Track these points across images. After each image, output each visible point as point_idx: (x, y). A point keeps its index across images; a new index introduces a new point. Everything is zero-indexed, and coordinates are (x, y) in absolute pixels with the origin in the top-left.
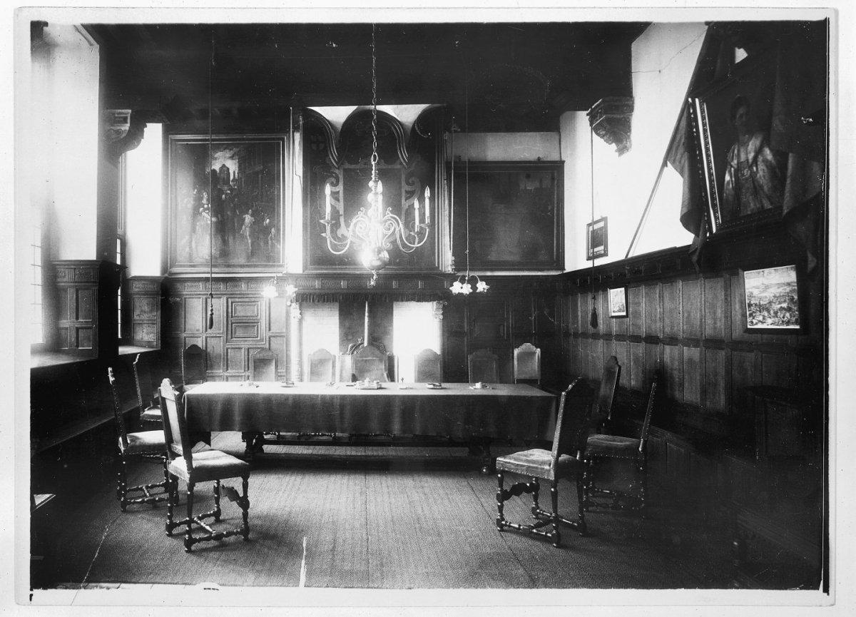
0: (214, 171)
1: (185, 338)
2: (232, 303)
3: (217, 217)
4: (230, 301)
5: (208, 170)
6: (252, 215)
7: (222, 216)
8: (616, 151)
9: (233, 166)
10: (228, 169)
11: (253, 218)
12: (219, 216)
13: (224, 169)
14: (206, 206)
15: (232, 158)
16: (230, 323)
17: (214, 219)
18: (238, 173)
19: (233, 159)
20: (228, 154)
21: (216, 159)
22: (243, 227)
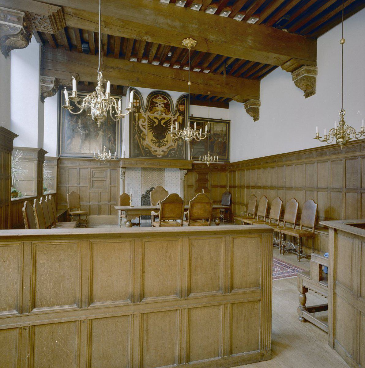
1: (69, 187)
2: (93, 171)
4: (91, 170)
8: (304, 96)
14: (80, 126)
17: (84, 132)
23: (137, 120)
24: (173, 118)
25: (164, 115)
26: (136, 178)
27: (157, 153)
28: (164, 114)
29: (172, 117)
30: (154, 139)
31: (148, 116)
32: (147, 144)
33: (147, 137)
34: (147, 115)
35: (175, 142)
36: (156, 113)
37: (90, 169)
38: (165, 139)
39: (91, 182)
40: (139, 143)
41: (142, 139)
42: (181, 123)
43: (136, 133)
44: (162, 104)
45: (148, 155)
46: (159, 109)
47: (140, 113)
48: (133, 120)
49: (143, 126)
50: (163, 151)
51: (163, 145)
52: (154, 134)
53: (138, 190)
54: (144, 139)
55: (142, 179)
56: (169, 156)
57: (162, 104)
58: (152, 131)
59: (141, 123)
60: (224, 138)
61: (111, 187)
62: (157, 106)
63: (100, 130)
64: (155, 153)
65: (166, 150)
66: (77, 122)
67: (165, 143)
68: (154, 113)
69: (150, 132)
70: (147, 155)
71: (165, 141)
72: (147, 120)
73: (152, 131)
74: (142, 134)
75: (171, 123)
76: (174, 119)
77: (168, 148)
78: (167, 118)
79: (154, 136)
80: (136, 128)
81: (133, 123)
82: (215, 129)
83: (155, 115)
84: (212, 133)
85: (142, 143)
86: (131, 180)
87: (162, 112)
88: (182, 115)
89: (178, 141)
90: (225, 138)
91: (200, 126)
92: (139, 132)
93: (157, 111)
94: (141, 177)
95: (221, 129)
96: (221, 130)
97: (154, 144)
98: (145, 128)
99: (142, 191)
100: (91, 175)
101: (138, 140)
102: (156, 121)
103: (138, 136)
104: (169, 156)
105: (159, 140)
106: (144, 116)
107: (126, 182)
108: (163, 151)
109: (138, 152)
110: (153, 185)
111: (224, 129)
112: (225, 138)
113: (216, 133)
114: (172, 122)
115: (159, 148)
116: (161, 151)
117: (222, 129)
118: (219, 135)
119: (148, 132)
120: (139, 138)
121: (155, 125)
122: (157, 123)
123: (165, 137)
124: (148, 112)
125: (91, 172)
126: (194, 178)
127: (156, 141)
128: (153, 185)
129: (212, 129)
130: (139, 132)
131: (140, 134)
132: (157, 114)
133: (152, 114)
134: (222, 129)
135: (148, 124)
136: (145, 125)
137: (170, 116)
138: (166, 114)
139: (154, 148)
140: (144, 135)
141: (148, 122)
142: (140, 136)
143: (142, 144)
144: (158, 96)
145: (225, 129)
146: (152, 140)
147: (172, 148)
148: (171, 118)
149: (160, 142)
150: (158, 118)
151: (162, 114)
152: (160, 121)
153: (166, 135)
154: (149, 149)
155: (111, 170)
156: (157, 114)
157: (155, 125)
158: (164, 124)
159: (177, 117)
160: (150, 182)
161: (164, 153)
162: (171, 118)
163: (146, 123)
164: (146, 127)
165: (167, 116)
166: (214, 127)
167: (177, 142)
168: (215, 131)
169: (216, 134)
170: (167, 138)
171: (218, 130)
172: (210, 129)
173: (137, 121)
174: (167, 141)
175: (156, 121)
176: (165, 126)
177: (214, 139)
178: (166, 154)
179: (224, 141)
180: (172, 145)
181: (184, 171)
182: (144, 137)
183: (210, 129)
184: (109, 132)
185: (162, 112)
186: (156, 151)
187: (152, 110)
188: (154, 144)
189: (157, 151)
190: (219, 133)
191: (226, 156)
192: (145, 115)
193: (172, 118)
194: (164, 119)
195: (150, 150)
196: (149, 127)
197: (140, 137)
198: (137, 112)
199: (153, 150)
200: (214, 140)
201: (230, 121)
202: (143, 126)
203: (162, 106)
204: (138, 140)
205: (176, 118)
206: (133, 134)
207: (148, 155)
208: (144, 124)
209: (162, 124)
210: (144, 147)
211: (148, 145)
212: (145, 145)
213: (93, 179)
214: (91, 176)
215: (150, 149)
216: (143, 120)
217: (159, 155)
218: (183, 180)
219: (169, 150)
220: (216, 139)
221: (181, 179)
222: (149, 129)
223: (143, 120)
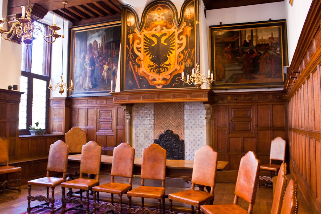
0: (91, 44)
2: (99, 111)
3: (92, 67)
4: (98, 110)
5: (88, 43)
6: (108, 65)
7: (94, 67)
9: (99, 41)
10: (97, 42)
11: (108, 67)
12: (93, 67)
13: (96, 42)
14: (87, 62)
15: (99, 36)
16: (98, 122)
17: (90, 69)
18: (102, 44)
19: (99, 37)
20: (97, 34)
21: (91, 38)
22: (103, 71)
23: (131, 42)
24: (178, 31)
25: (165, 30)
27: (156, 82)
28: (164, 28)
29: (176, 30)
30: (152, 63)
31: (144, 35)
32: (143, 72)
33: (142, 63)
34: (143, 34)
35: (182, 64)
36: (154, 29)
37: (97, 108)
38: (167, 63)
39: (98, 123)
40: (134, 72)
41: (136, 66)
42: (189, 35)
43: (130, 60)
44: (162, 15)
45: (145, 86)
46: (159, 23)
47: (135, 33)
48: (127, 44)
49: (138, 49)
50: (164, 79)
51: (164, 70)
52: (152, 57)
53: (149, 134)
54: (139, 66)
55: (154, 120)
56: (173, 85)
57: (162, 15)
58: (150, 54)
59: (135, 45)
60: (277, 49)
62: (156, 20)
63: (105, 64)
64: (153, 82)
65: (169, 77)
66: (84, 58)
67: (166, 68)
68: (151, 30)
69: (147, 55)
70: (143, 86)
71: (167, 65)
72: (143, 41)
73: (150, 54)
74: (137, 59)
75: (175, 39)
76: (179, 32)
77: (171, 74)
78: (169, 33)
79: (152, 60)
80: (130, 52)
81: (127, 48)
82: (260, 38)
83: (153, 32)
84: (254, 44)
85: (136, 71)
87: (162, 26)
88: (190, 25)
89: (185, 62)
90: (278, 49)
91: (235, 36)
92: (134, 58)
93: (156, 26)
95: (270, 36)
96: (270, 38)
97: (152, 71)
98: (140, 52)
99: (154, 135)
101: (132, 68)
102: (154, 39)
103: (132, 63)
104: (173, 85)
105: (159, 64)
106: (140, 36)
108: (164, 79)
109: (132, 84)
110: (169, 126)
111: (276, 35)
112: (278, 49)
113: (261, 43)
114: (176, 37)
115: (159, 75)
116: (161, 79)
117: (272, 35)
118: (267, 45)
119: (144, 56)
120: (133, 65)
121: (153, 45)
122: (156, 43)
123: (166, 59)
124: (145, 30)
126: (227, 117)
127: (154, 66)
128: (169, 126)
129: (254, 39)
130: (134, 58)
131: (135, 60)
132: (156, 30)
133: (150, 32)
134: (272, 35)
135: (145, 46)
136: (140, 48)
137: (173, 29)
138: (167, 28)
139: (152, 75)
140: (140, 60)
141: (144, 42)
142: (135, 62)
143: (137, 73)
144: (157, 7)
145: (277, 36)
146: (149, 66)
147: (176, 73)
148: (174, 32)
149: (159, 67)
150: (157, 34)
151: (162, 29)
152: (159, 39)
153: (168, 56)
154: (144, 78)
156: (156, 30)
157: (153, 45)
158: (165, 41)
159: (183, 29)
160: (165, 123)
161: (165, 81)
162: (174, 32)
163: (142, 45)
164: (142, 50)
165: (169, 30)
166: (257, 34)
167: (183, 63)
168: (260, 40)
169: (262, 45)
170: (170, 60)
171: (264, 38)
172: (250, 39)
173: (131, 44)
174: (169, 65)
175: (154, 39)
176: (166, 44)
177: (259, 53)
178: (169, 82)
179: (277, 53)
180: (176, 70)
181: (205, 105)
182: (140, 64)
183: (250, 39)
184: (114, 64)
185: (162, 26)
186: (154, 80)
187: (148, 27)
188: (152, 71)
189: (156, 80)
190: (266, 43)
191: (282, 78)
192: (141, 34)
193: (176, 32)
194: (164, 35)
195: (147, 80)
196: (145, 49)
197: (135, 63)
198: (131, 34)
199: (150, 79)
200: (258, 55)
201: (285, 20)
202: (138, 49)
203: (162, 19)
204: (132, 68)
205: (181, 30)
206: (127, 61)
207: (145, 86)
208: (140, 46)
209: (162, 42)
210: (139, 76)
211: (145, 73)
212: (140, 73)
213: (100, 121)
214: (98, 117)
215: (147, 78)
216: (138, 41)
217: (159, 85)
218: (208, 119)
219: (172, 77)
220: (262, 52)
221: (206, 118)
222: (145, 52)
223: (138, 41)
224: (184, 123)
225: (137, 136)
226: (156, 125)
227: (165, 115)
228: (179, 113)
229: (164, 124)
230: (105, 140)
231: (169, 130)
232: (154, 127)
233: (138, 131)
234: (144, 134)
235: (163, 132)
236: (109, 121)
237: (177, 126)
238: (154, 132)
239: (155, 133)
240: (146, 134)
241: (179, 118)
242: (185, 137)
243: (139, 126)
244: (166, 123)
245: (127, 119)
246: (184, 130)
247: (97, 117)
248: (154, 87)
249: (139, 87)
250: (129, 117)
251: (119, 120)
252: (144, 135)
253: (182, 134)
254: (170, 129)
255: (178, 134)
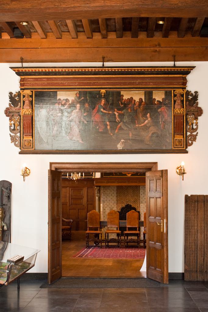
2: (71, 190)
16: (70, 198)
26: (111, 195)
61: (88, 204)
86: (106, 197)
94: (116, 195)
99: (117, 208)
100: (70, 193)
107: (102, 199)
125: (70, 190)
155: (87, 188)
160: (125, 199)
214: (70, 195)
217: (129, 174)
224: (140, 199)
225: (104, 209)
226: (118, 201)
227: (125, 193)
228: (136, 192)
229: (124, 199)
230: (77, 213)
231: (128, 205)
232: (117, 202)
233: (105, 205)
234: (110, 208)
235: (124, 206)
236: (81, 197)
237: (135, 201)
238: (117, 206)
239: (118, 207)
240: (111, 207)
241: (136, 195)
242: (141, 209)
243: (106, 202)
244: (126, 199)
245: (97, 196)
246: (140, 204)
247: (69, 194)
248: (125, 175)
249: (114, 175)
250: (99, 195)
251: (89, 197)
252: (109, 209)
253: (138, 207)
254: (130, 204)
255: (135, 207)
